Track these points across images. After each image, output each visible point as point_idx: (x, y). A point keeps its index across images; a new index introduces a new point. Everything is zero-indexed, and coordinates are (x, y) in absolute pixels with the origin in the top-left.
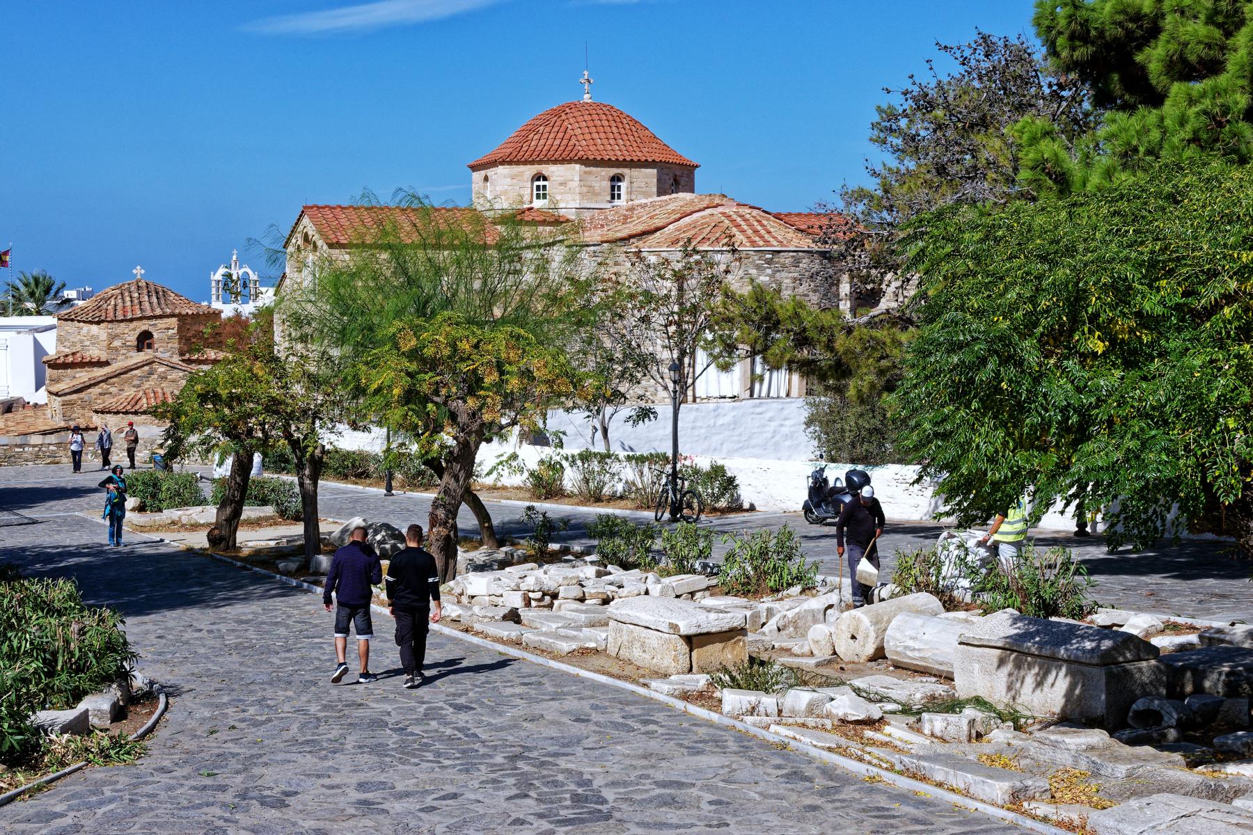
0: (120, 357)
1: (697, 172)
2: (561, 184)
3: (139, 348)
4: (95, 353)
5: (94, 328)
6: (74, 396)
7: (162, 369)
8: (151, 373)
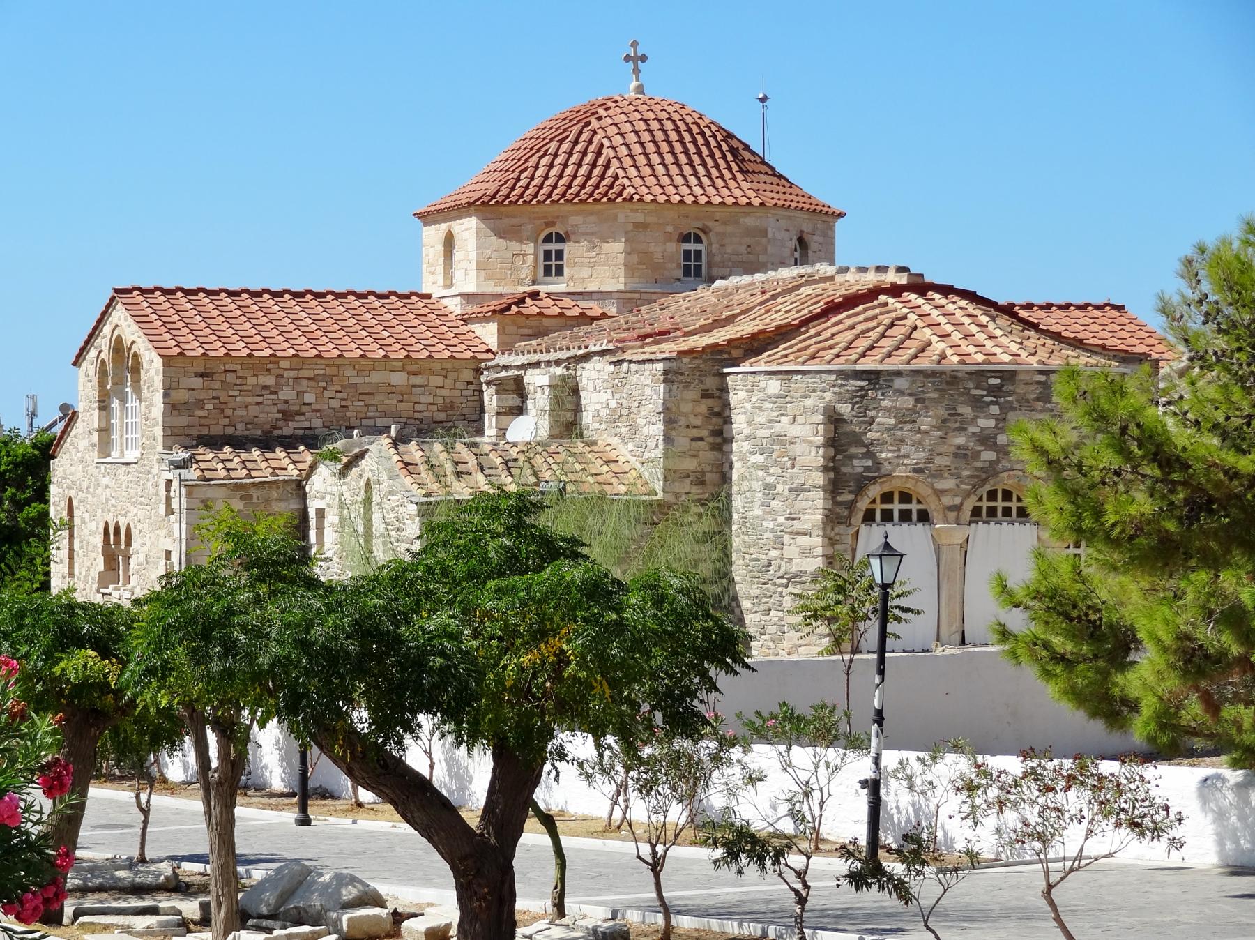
1: (840, 224)
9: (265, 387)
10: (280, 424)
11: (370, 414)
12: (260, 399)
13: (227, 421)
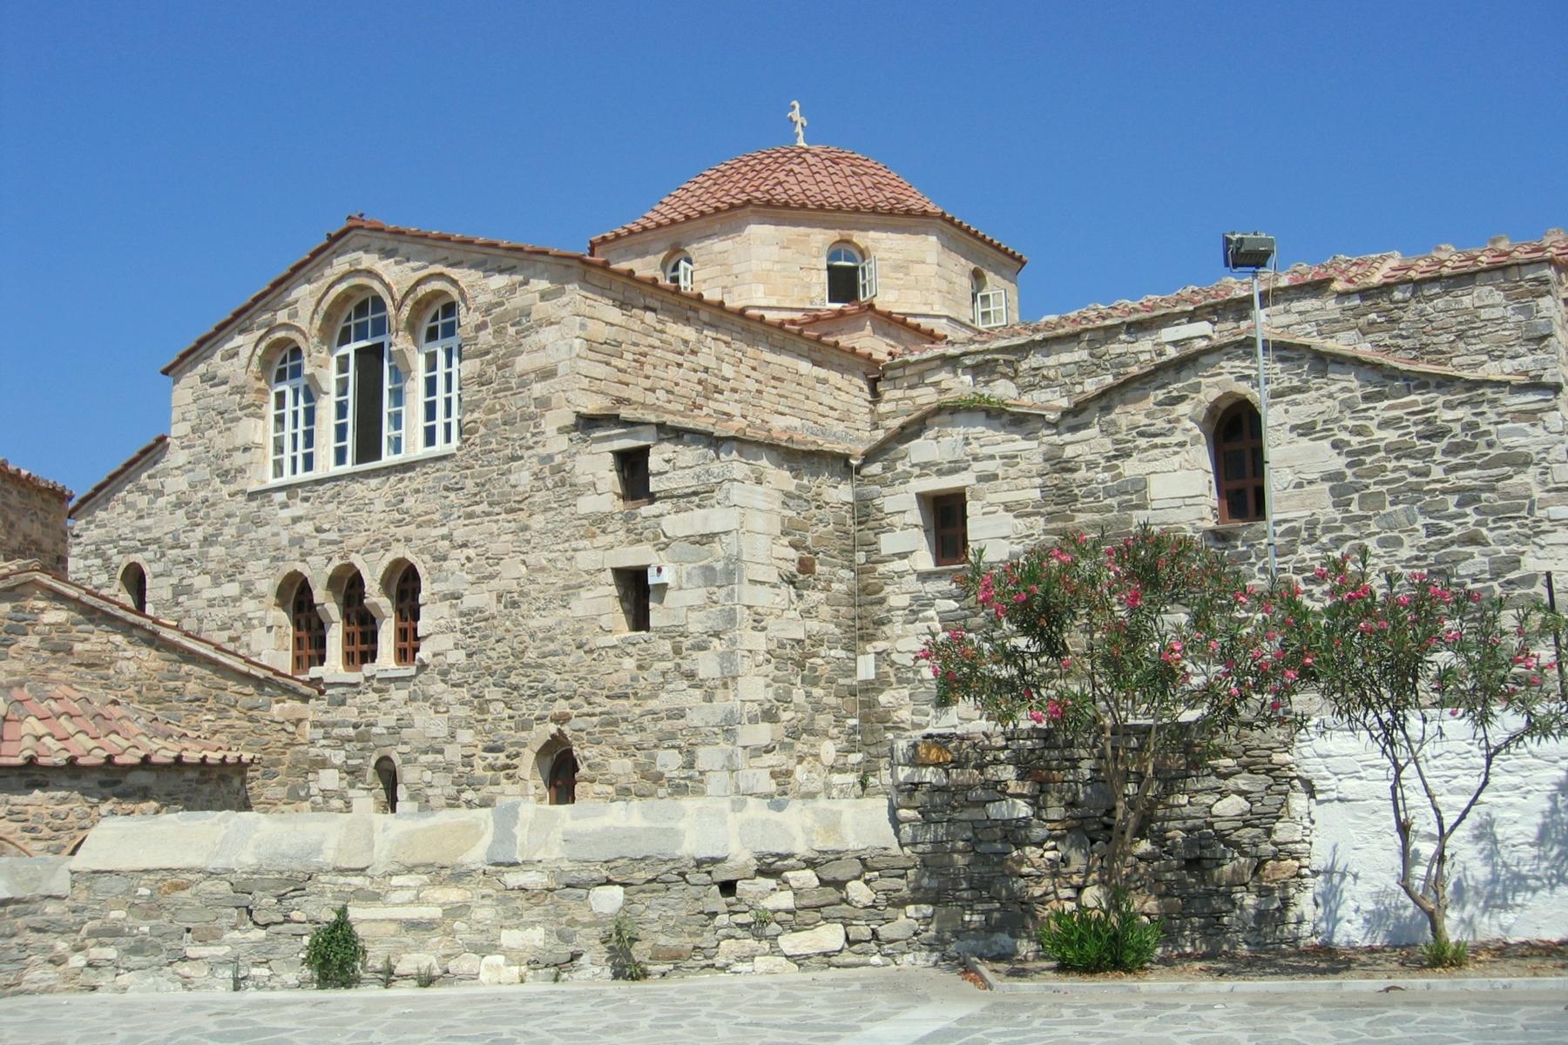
7: (56, 615)
9: (686, 342)
10: (700, 401)
11: (781, 409)
12: (680, 359)
13: (648, 383)
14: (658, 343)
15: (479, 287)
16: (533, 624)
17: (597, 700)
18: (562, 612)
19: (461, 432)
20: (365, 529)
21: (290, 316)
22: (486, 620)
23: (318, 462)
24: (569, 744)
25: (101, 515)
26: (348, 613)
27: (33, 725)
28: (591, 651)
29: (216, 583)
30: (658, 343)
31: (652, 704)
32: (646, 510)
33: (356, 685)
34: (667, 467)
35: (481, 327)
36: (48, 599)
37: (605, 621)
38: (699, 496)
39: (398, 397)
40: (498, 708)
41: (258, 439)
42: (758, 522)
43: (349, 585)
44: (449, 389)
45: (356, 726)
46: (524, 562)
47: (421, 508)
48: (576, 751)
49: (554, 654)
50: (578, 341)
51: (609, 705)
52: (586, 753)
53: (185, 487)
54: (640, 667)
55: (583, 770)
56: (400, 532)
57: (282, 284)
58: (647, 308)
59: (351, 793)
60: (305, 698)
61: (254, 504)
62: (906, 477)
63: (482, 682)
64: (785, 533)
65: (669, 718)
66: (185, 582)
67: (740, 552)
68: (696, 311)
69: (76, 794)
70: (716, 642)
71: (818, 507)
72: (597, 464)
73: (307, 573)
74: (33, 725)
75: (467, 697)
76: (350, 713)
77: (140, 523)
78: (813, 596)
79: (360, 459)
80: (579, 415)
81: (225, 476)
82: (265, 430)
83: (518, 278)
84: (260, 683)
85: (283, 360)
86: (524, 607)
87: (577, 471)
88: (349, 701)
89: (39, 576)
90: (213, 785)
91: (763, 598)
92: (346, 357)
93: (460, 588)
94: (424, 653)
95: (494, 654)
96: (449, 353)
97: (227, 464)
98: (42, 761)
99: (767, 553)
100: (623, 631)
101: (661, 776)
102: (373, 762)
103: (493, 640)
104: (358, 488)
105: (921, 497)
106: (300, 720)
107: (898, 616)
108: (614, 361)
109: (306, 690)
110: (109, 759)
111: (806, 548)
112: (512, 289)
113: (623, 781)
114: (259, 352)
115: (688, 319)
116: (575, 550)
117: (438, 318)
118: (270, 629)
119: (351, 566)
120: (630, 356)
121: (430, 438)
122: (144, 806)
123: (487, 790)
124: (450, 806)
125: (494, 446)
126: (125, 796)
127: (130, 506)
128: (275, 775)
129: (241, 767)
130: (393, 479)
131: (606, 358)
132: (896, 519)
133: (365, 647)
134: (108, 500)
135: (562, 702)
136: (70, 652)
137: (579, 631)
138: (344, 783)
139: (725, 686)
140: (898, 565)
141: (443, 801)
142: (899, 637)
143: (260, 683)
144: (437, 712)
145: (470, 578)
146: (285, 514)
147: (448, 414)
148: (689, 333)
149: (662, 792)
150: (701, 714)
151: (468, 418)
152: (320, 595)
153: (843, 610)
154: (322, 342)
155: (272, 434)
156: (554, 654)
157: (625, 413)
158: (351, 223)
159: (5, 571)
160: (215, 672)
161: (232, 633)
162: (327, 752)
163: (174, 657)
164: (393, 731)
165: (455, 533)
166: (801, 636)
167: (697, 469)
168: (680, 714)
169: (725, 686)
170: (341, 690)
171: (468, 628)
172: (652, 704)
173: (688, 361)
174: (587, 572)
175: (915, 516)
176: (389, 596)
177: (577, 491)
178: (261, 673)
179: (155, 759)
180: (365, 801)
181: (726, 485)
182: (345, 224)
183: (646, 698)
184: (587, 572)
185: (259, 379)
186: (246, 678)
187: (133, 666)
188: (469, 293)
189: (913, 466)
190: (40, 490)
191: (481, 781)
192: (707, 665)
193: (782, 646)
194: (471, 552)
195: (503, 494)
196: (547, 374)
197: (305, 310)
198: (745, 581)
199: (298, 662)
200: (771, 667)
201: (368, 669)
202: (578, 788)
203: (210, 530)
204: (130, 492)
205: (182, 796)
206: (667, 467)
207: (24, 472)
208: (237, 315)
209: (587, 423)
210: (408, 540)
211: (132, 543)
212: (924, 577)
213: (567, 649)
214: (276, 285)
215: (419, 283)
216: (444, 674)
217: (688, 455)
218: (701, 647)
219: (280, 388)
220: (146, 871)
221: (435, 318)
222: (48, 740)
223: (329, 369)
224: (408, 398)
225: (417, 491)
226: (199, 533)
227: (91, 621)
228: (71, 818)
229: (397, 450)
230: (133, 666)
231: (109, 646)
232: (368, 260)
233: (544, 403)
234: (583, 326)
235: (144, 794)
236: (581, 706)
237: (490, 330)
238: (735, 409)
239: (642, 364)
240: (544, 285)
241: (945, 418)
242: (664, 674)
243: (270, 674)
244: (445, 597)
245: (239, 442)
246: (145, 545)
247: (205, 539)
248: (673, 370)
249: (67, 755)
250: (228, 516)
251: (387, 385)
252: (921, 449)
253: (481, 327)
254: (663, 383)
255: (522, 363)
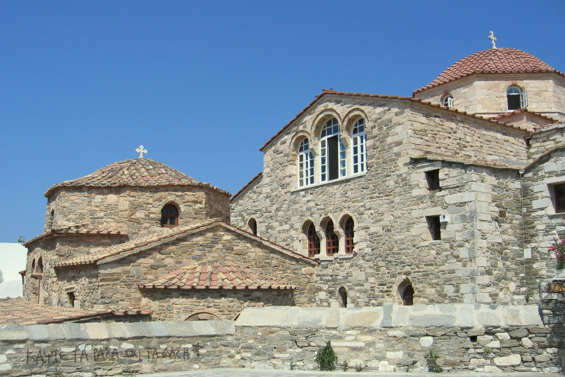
0: (142, 232)
2: (536, 94)
3: (163, 222)
4: (110, 226)
5: (112, 198)
6: (119, 270)
8: (215, 241)
9: (452, 129)
12: (450, 135)
13: (438, 145)
14: (441, 130)
15: (372, 112)
16: (396, 238)
17: (421, 266)
18: (407, 233)
19: (367, 167)
20: (334, 204)
21: (304, 127)
22: (379, 236)
23: (315, 180)
24: (411, 283)
25: (241, 202)
26: (329, 235)
27: (221, 275)
28: (418, 248)
29: (281, 225)
30: (441, 130)
31: (442, 268)
32: (438, 194)
33: (331, 261)
34: (446, 177)
35: (373, 127)
36: (224, 231)
37: (423, 236)
38: (459, 188)
39: (344, 155)
40: (384, 269)
41: (294, 173)
42: (483, 197)
43: (328, 224)
44: (362, 151)
45: (331, 276)
46: (392, 215)
47: (353, 196)
48: (413, 285)
49: (404, 249)
50: (410, 131)
51: (425, 268)
52: (417, 286)
53: (269, 191)
54: (437, 254)
55: (416, 293)
56: (346, 205)
57: (300, 116)
58: (436, 117)
59: (330, 300)
60: (314, 266)
61: (293, 196)
62: (543, 178)
63: (377, 260)
64: (493, 201)
65: (449, 273)
66: (270, 225)
67: (476, 209)
68: (455, 116)
69: (236, 299)
70: (467, 244)
71: (507, 191)
72: (419, 177)
73: (313, 220)
74: (221, 275)
75: (372, 265)
76: (329, 271)
77: (254, 204)
78: (506, 226)
79: (331, 178)
80: (411, 159)
81: (283, 186)
82: (296, 169)
83: (386, 108)
84: (297, 261)
85: (302, 144)
86: (393, 231)
87: (411, 180)
88: (329, 267)
89: (222, 224)
90: (282, 297)
91: (485, 227)
92: (324, 141)
93: (368, 225)
94: (356, 249)
95: (382, 249)
96: (362, 138)
97: (283, 182)
98: (224, 287)
99: (486, 209)
100: (431, 240)
101: (446, 295)
102: (338, 289)
103: (381, 244)
104: (330, 189)
105: (550, 186)
106: (312, 274)
107: (541, 233)
108: (424, 138)
109: (314, 263)
110: (247, 287)
111: (502, 207)
112: (384, 112)
113: (431, 297)
114: (293, 141)
115: (452, 120)
116: (411, 210)
117: (357, 125)
118: (300, 241)
119: (329, 217)
120: (430, 135)
121: (356, 170)
122: (259, 304)
123: (380, 300)
124: (366, 305)
125: (380, 172)
126: (252, 300)
127: (250, 198)
128: (304, 293)
129: (292, 290)
130: (343, 185)
131: (421, 137)
132: (539, 195)
133: (334, 247)
134: (243, 196)
135: (408, 267)
136: (232, 250)
137: (414, 240)
138: (328, 297)
139: (471, 261)
140: (540, 213)
141: (364, 304)
142: (541, 241)
143: (297, 261)
144: (361, 271)
145: (372, 221)
146: (305, 199)
147: (362, 160)
148: (453, 125)
149: (446, 301)
150: (461, 271)
151: (370, 162)
152: (318, 228)
153: (518, 231)
154: (315, 136)
155: (299, 171)
156: (404, 249)
157: (429, 157)
158: (324, 92)
159: (210, 222)
160: (282, 256)
161: (287, 242)
162: (322, 285)
163: (268, 251)
164: (345, 278)
165: (366, 205)
166: (501, 241)
167: (458, 178)
168: (453, 272)
169: (471, 261)
170: (326, 263)
171: (372, 240)
172: (442, 268)
173: (453, 136)
174: (416, 218)
175: (547, 193)
176: (343, 228)
177: (412, 187)
178: (298, 257)
179: (262, 287)
180: (335, 303)
181: (470, 183)
182: (321, 93)
183: (440, 265)
184: (416, 218)
185: (293, 151)
186: (292, 258)
187: (254, 255)
188: (368, 115)
189: (545, 173)
190: (221, 194)
191: (378, 296)
192: (463, 253)
193: (493, 245)
194: (372, 211)
195: (383, 190)
196: (399, 144)
197: (309, 125)
198: (478, 220)
199: (310, 252)
200: (489, 253)
201: (336, 255)
202: (414, 300)
203: (278, 206)
204: (250, 193)
205: (271, 301)
206: (446, 177)
207: (215, 188)
208: (285, 128)
209: (415, 161)
210: (349, 207)
211: (252, 211)
212: (551, 217)
213: (409, 247)
214: (298, 116)
215: (350, 112)
216: (363, 257)
217: (454, 172)
218: (461, 246)
219: (301, 154)
220: (260, 327)
221: (356, 125)
222: (226, 280)
223: (318, 146)
224: (347, 155)
225: (352, 189)
226: (275, 207)
227: (239, 239)
228: (234, 308)
229: (344, 175)
230: (254, 255)
231: (246, 248)
232: (331, 105)
233: (398, 155)
234: (412, 125)
235: (258, 300)
236: (415, 269)
237: (377, 128)
238: (472, 154)
239: (435, 138)
240: (396, 110)
241: (559, 153)
242: (447, 256)
243: (301, 257)
244: (363, 228)
245: (287, 174)
246: (256, 212)
247: (277, 209)
248: (447, 139)
249: (232, 286)
250: (285, 201)
251: (339, 151)
252: (549, 166)
253: (373, 127)
254: (443, 145)
255: (389, 140)
